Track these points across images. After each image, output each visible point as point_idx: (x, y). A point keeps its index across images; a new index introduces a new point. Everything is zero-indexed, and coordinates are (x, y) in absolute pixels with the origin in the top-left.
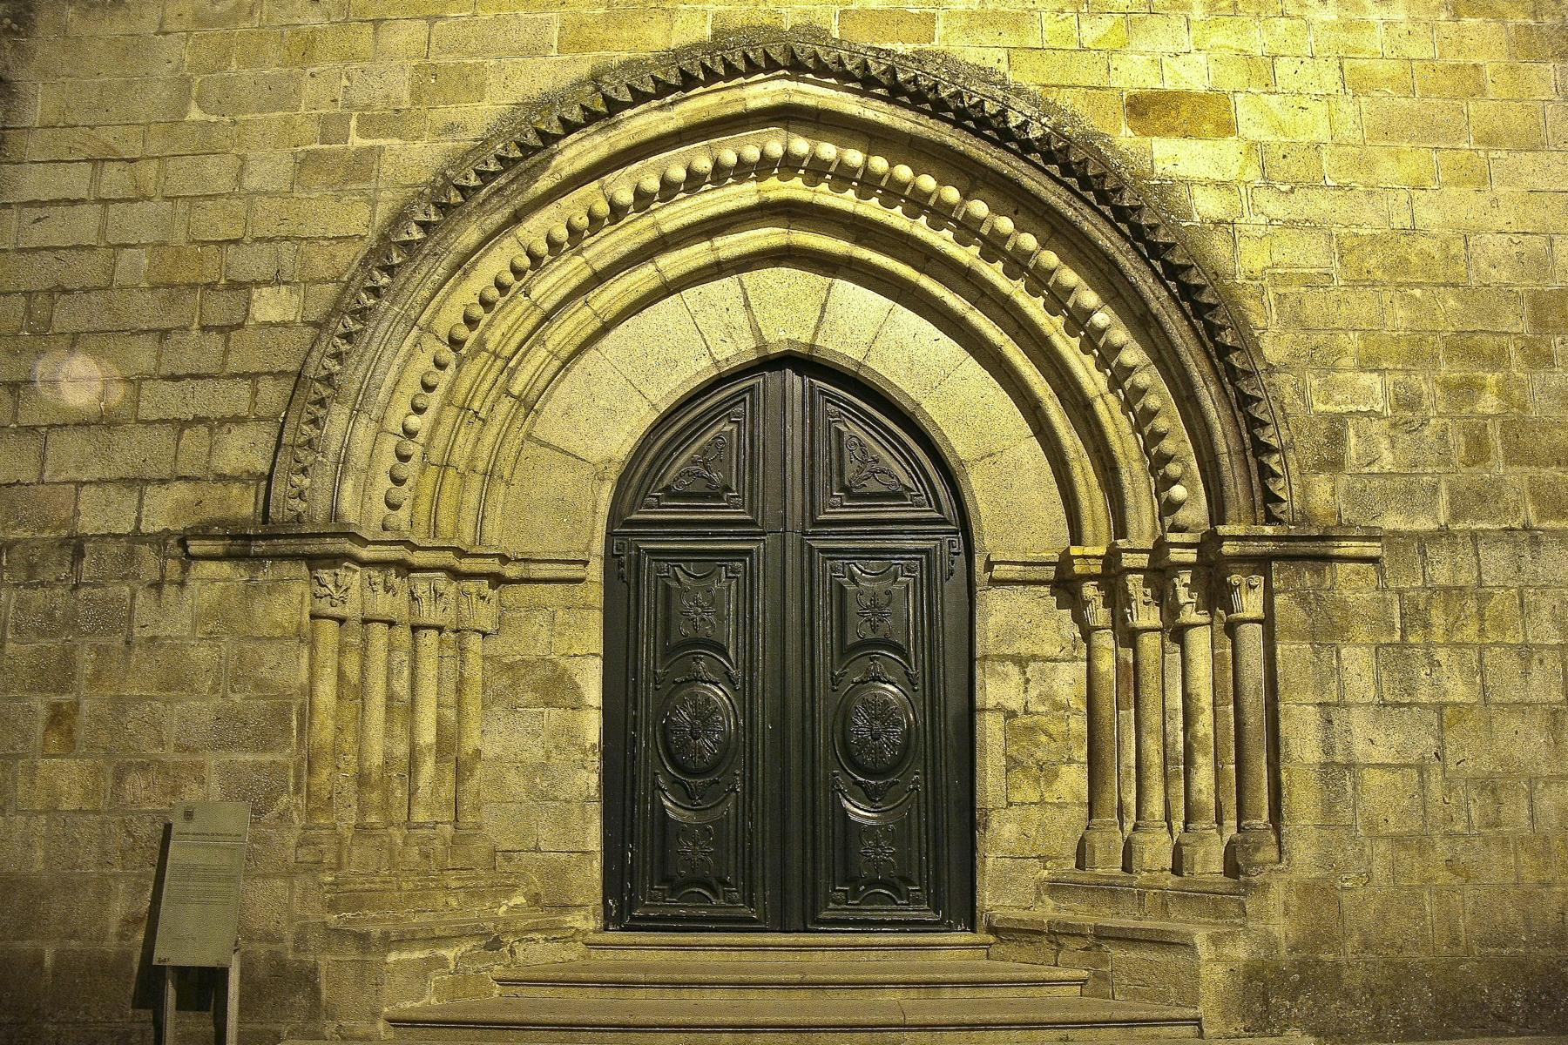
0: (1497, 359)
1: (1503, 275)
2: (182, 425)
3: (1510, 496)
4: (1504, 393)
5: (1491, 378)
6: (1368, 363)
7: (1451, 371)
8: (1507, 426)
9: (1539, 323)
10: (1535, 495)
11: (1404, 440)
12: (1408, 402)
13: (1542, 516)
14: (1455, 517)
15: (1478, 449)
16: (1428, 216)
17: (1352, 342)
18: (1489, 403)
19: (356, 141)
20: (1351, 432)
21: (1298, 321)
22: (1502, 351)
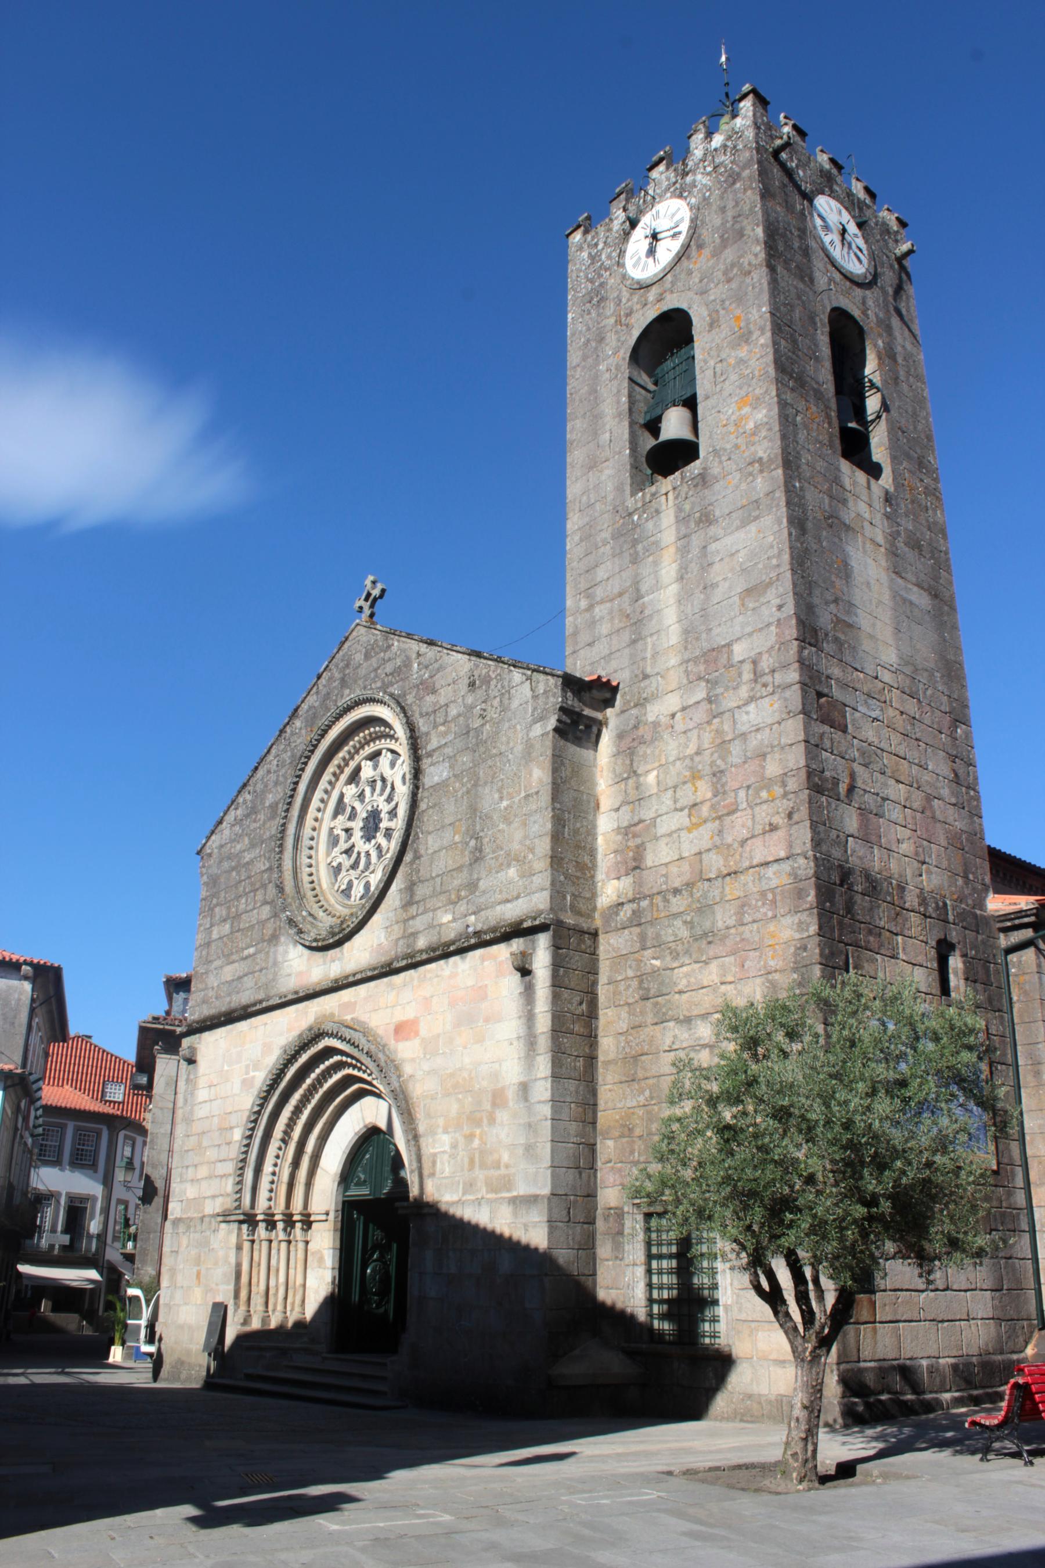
0: (478, 1123)
1: (485, 1083)
2: (222, 1177)
3: (479, 1184)
4: (481, 1139)
5: (478, 1131)
6: (446, 1131)
7: (466, 1130)
8: (481, 1152)
9: (494, 1104)
10: (486, 1183)
11: (452, 1161)
12: (454, 1146)
13: (487, 1192)
14: (464, 1194)
15: (472, 1161)
16: (467, 1060)
17: (441, 1121)
18: (476, 1143)
19: (252, 1074)
20: (438, 1161)
21: (428, 1116)
22: (481, 1119)
